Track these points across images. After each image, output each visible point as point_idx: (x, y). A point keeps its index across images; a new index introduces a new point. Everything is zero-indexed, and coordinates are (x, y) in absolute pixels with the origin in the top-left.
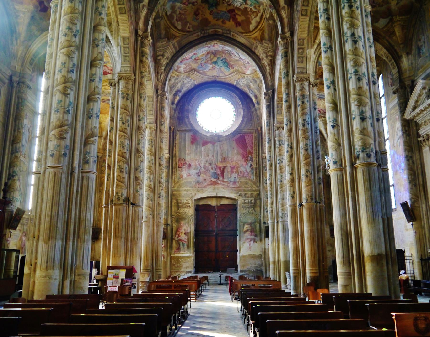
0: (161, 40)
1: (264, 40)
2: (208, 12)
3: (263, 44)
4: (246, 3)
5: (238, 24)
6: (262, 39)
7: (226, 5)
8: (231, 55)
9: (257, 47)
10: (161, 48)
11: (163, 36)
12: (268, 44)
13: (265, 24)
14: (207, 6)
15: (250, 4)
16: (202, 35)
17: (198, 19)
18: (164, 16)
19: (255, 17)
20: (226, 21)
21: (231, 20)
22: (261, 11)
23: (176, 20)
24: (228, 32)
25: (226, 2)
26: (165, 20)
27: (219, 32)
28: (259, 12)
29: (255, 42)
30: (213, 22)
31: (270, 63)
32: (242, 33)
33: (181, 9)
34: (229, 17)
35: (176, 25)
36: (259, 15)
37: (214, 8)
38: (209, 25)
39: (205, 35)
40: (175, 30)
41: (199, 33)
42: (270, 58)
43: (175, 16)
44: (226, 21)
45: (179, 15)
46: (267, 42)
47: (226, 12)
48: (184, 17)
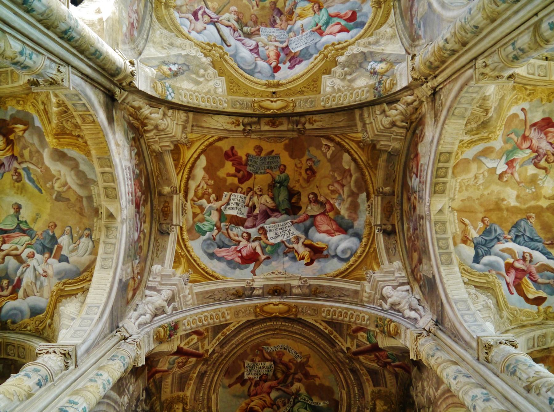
0: (390, 150)
1: (171, 150)
2: (289, 171)
3: (172, 142)
4: (219, 211)
5: (231, 155)
6: (176, 151)
7: (255, 189)
8: (238, 20)
9: (184, 128)
10: (393, 136)
11: (384, 157)
12: (161, 147)
13: (176, 180)
14: (291, 184)
15: (212, 211)
16: (303, 120)
17: (308, 160)
18: (374, 193)
19: (199, 186)
20: (253, 153)
21: (244, 158)
22: (189, 204)
23: (351, 176)
24: (249, 128)
25: (256, 193)
26: (372, 184)
27: (267, 124)
28: (193, 200)
29: (189, 136)
30: (279, 148)
31: (146, 121)
32: (220, 139)
33: (340, 194)
34: (249, 163)
35: (353, 166)
36: (191, 195)
37: (277, 178)
38: (287, 141)
39: (295, 118)
40: (356, 156)
41: (308, 126)
42: (149, 127)
43: (352, 184)
44: (253, 153)
45: (344, 182)
46: (163, 149)
47: (256, 173)
48: (336, 175)
